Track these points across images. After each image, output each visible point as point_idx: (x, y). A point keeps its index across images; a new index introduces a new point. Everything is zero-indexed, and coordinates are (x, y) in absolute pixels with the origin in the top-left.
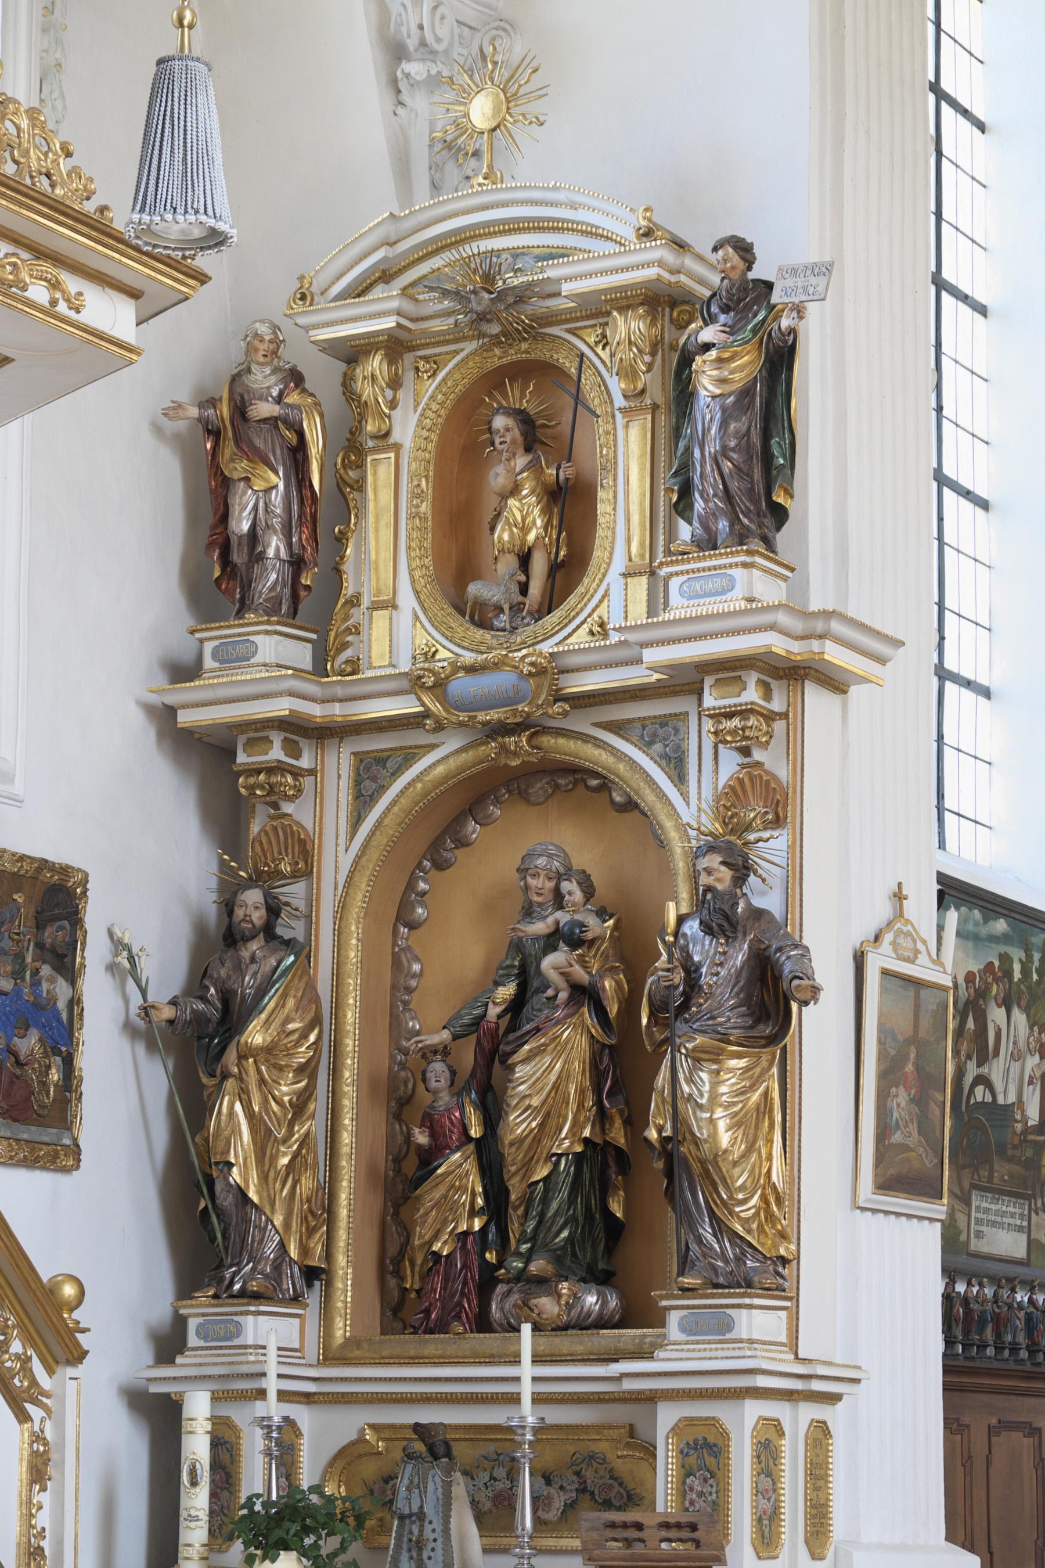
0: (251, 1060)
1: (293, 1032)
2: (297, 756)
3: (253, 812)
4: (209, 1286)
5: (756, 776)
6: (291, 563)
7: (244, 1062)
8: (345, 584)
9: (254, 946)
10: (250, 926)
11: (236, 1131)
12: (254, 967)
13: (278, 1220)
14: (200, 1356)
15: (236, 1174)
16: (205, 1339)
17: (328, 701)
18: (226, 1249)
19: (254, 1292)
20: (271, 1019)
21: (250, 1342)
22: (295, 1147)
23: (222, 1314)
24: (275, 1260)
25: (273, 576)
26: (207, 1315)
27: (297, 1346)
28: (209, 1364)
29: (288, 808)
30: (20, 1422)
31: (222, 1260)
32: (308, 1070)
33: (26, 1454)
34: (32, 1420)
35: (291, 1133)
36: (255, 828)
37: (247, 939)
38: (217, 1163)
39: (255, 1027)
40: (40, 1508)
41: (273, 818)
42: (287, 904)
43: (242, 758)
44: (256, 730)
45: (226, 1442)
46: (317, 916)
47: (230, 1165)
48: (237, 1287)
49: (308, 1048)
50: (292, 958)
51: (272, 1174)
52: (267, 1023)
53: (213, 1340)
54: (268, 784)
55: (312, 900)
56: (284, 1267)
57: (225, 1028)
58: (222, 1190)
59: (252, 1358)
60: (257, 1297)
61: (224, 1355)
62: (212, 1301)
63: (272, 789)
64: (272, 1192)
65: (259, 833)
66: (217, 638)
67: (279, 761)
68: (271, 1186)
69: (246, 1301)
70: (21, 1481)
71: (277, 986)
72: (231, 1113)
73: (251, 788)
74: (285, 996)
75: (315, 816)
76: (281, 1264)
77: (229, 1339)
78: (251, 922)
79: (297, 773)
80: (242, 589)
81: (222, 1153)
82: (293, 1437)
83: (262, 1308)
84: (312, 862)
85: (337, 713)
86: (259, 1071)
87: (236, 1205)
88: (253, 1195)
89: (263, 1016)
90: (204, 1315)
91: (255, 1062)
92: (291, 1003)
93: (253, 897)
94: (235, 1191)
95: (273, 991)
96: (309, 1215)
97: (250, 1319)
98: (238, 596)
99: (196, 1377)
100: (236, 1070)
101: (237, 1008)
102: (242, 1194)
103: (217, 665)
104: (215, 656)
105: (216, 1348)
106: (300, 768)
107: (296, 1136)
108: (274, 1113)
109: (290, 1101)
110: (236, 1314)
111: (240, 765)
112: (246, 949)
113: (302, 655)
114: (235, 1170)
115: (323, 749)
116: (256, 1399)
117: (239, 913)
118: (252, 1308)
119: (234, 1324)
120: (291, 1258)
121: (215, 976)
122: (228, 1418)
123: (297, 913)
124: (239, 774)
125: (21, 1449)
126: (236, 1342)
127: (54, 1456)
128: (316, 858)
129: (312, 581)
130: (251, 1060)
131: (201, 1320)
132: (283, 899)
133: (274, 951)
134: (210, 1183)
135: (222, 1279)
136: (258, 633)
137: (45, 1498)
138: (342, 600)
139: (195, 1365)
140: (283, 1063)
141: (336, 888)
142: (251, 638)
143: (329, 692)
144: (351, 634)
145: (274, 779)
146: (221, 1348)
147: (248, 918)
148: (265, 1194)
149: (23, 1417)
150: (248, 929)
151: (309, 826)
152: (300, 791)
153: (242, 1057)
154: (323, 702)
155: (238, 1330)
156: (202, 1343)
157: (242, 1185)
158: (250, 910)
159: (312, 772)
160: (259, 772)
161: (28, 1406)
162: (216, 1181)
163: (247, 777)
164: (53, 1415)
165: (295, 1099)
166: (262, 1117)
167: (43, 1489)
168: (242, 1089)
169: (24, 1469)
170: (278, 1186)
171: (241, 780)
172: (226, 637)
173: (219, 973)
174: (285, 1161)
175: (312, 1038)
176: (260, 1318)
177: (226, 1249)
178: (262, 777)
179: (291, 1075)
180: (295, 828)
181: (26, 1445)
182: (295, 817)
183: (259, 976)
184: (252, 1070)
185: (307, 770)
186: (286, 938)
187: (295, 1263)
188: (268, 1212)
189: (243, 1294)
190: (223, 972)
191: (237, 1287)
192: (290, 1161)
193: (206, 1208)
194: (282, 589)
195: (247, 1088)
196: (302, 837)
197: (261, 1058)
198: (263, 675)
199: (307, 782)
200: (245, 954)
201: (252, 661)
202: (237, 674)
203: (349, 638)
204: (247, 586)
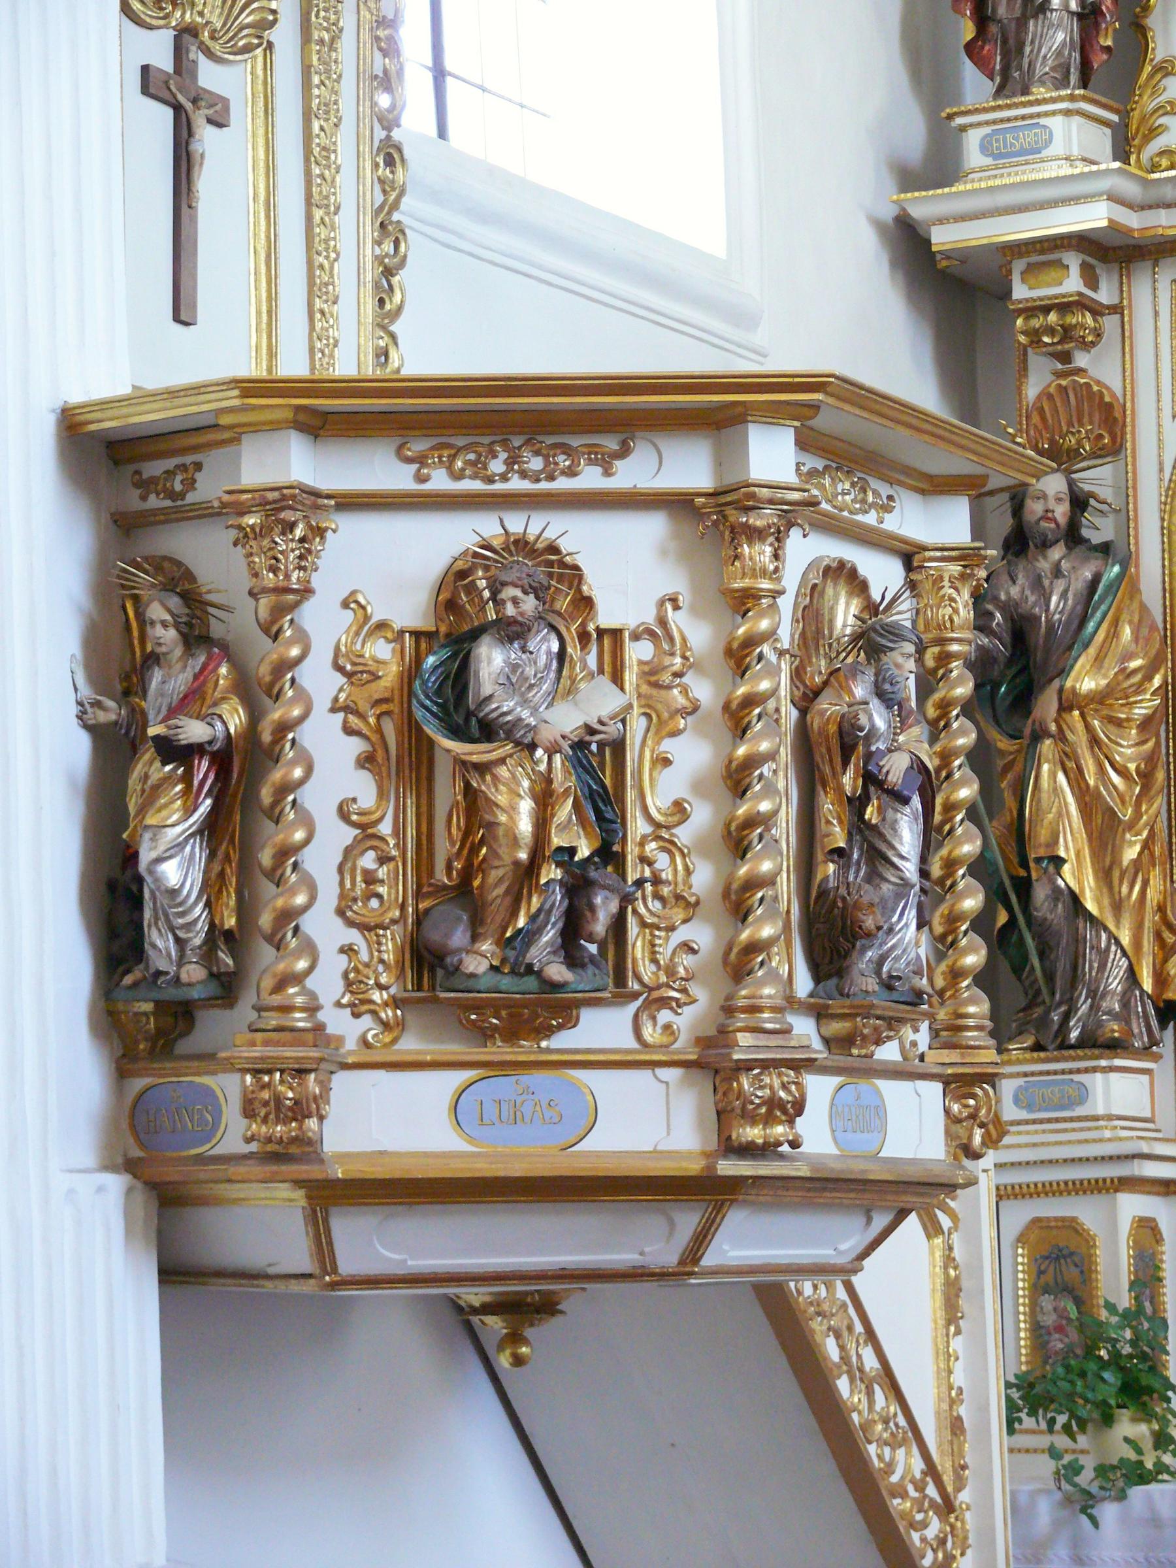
0: (1076, 713)
1: (1135, 672)
2: (1095, 288)
3: (1025, 369)
4: (1020, 1033)
5: (1081, 385)
6: (1080, 16)
7: (1064, 715)
8: (1151, 45)
9: (1057, 553)
10: (1053, 525)
11: (1063, 813)
12: (1060, 585)
13: (1126, 939)
14: (1028, 1133)
15: (1068, 876)
16: (1029, 1108)
17: (1150, 207)
18: (1050, 977)
19: (1115, 1039)
20: (1102, 654)
21: (1100, 1111)
22: (1145, 834)
23: (1055, 1073)
24: (1124, 993)
25: (1060, 36)
26: (1033, 1074)
27: (1149, 1115)
28: (1048, 1144)
29: (1081, 360)
30: (929, 1237)
31: (1038, 992)
32: (1146, 724)
33: (940, 1281)
34: (943, 1233)
35: (1138, 814)
36: (1031, 391)
37: (1045, 545)
38: (1038, 860)
39: (1083, 666)
40: (957, 1359)
41: (1059, 375)
42: (1092, 495)
43: (1020, 292)
44: (1042, 252)
45: (1072, 1254)
46: (1136, 510)
47: (1058, 862)
48: (1074, 1035)
49: (1153, 694)
50: (1116, 569)
51: (1116, 874)
52: (1099, 660)
53: (1047, 1110)
54: (1062, 326)
55: (1128, 489)
56: (1133, 1004)
57: (1014, 670)
58: (1047, 896)
59: (1107, 1134)
60: (1114, 1046)
61: (1065, 1131)
62: (1028, 1055)
63: (1067, 333)
64: (1117, 897)
65: (1039, 398)
66: (987, 123)
67: (1080, 294)
68: (1116, 889)
69: (1097, 1052)
70: (935, 1322)
71: (1103, 607)
72: (1056, 790)
73: (1034, 336)
74: (1116, 623)
75: (1124, 371)
76: (1129, 1001)
77: (1070, 1105)
78: (1055, 521)
79: (1097, 311)
80: (1005, 55)
81: (1048, 846)
82: (1154, 1242)
83: (1118, 1062)
84: (1123, 434)
85: (1164, 223)
86: (1088, 728)
87: (1066, 918)
88: (1090, 905)
89: (1092, 651)
90: (1026, 1075)
91: (1082, 715)
92: (1127, 632)
93: (1054, 485)
94: (1067, 897)
95: (1098, 615)
96: (1163, 928)
97: (1098, 1076)
98: (998, 67)
99: (1028, 1163)
100: (1053, 727)
101: (1041, 641)
102: (1075, 900)
103: (989, 161)
104: (985, 148)
105: (1049, 1121)
106: (1101, 304)
107: (1145, 817)
108: (1115, 787)
109: (1137, 769)
110: (1079, 1071)
111: (1020, 302)
112: (1045, 557)
113: (1100, 141)
114: (1066, 869)
115: (1128, 277)
116: (1116, 1191)
117: (1034, 508)
118: (1103, 1063)
119: (1073, 1085)
120: (1142, 991)
121: (1003, 597)
122: (1074, 1219)
123: (1104, 507)
124: (1020, 312)
125: (933, 1275)
126: (1079, 1111)
127: (965, 1284)
128: (1129, 429)
129: (1114, 40)
130: (1076, 713)
131: (1021, 1081)
132: (1087, 487)
133: (1087, 559)
134: (1024, 887)
135: (1043, 1022)
136: (1054, 113)
137: (957, 1344)
138: (1148, 69)
139: (1027, 1145)
140: (1123, 716)
141: (1161, 470)
142: (1043, 121)
143: (1154, 194)
144: (1166, 113)
145: (1071, 320)
146: (1057, 1120)
147: (1050, 515)
148: (1106, 901)
149: (932, 1228)
150: (1050, 529)
151: (1117, 387)
152: (1099, 335)
153: (1065, 707)
154: (1142, 208)
155: (1082, 1094)
156: (1024, 1115)
157: (1077, 891)
158: (1052, 504)
159: (1117, 309)
160: (1047, 310)
161: (937, 1211)
162: (1035, 884)
163: (1027, 319)
164: (960, 1225)
165: (1143, 766)
166: (1099, 793)
167: (958, 1332)
168: (1066, 754)
169: (938, 1304)
170: (1125, 890)
171: (1019, 322)
172: (1002, 121)
173: (1008, 593)
174: (1131, 853)
175: (1157, 681)
176: (1113, 1076)
177: (1050, 977)
178: (1053, 317)
179: (1134, 732)
180: (1095, 388)
181: (938, 1270)
182: (1091, 372)
183: (1070, 595)
184: (1080, 726)
185: (1108, 307)
186: (1094, 542)
187: (1149, 996)
188: (1111, 926)
189: (1081, 1044)
190: (1015, 591)
191: (1074, 1035)
192: (1140, 854)
193: (1012, 922)
194: (1070, 55)
195: (1074, 752)
196: (1107, 399)
197: (1089, 712)
198: (1062, 173)
199: (1110, 323)
200: (1044, 565)
201: (1044, 153)
202: (1002, 176)
203: (1162, 121)
204: (1013, 50)
